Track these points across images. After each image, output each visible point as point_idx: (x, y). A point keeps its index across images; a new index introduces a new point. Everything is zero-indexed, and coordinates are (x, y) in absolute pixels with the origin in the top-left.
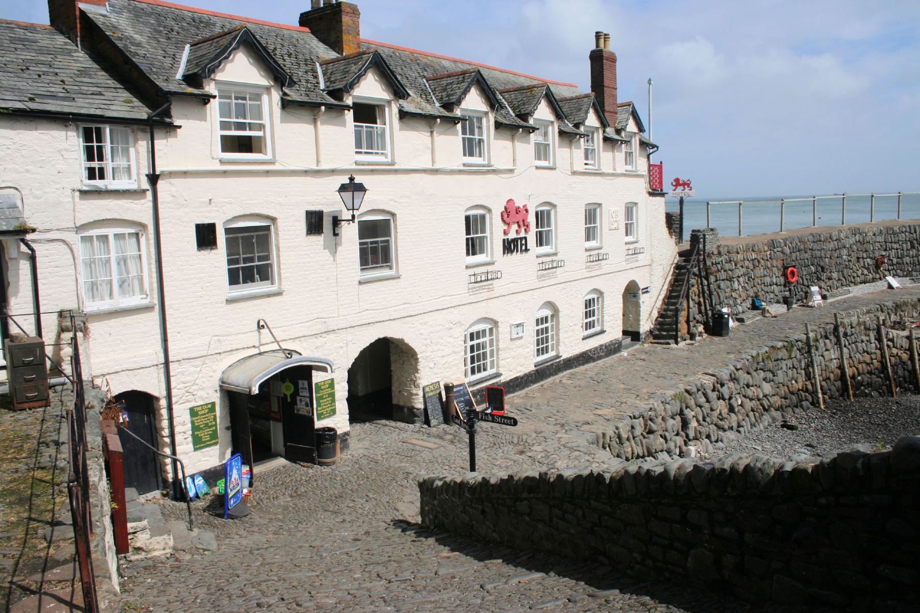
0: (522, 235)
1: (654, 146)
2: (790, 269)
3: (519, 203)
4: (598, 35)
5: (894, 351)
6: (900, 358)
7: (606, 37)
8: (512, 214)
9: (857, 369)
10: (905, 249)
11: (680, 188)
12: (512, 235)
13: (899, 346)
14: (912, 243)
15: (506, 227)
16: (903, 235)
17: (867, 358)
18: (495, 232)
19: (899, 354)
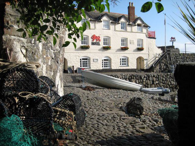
4: (130, 3)
7: (132, 3)
8: (94, 37)
11: (172, 39)
12: (95, 41)
18: (90, 41)
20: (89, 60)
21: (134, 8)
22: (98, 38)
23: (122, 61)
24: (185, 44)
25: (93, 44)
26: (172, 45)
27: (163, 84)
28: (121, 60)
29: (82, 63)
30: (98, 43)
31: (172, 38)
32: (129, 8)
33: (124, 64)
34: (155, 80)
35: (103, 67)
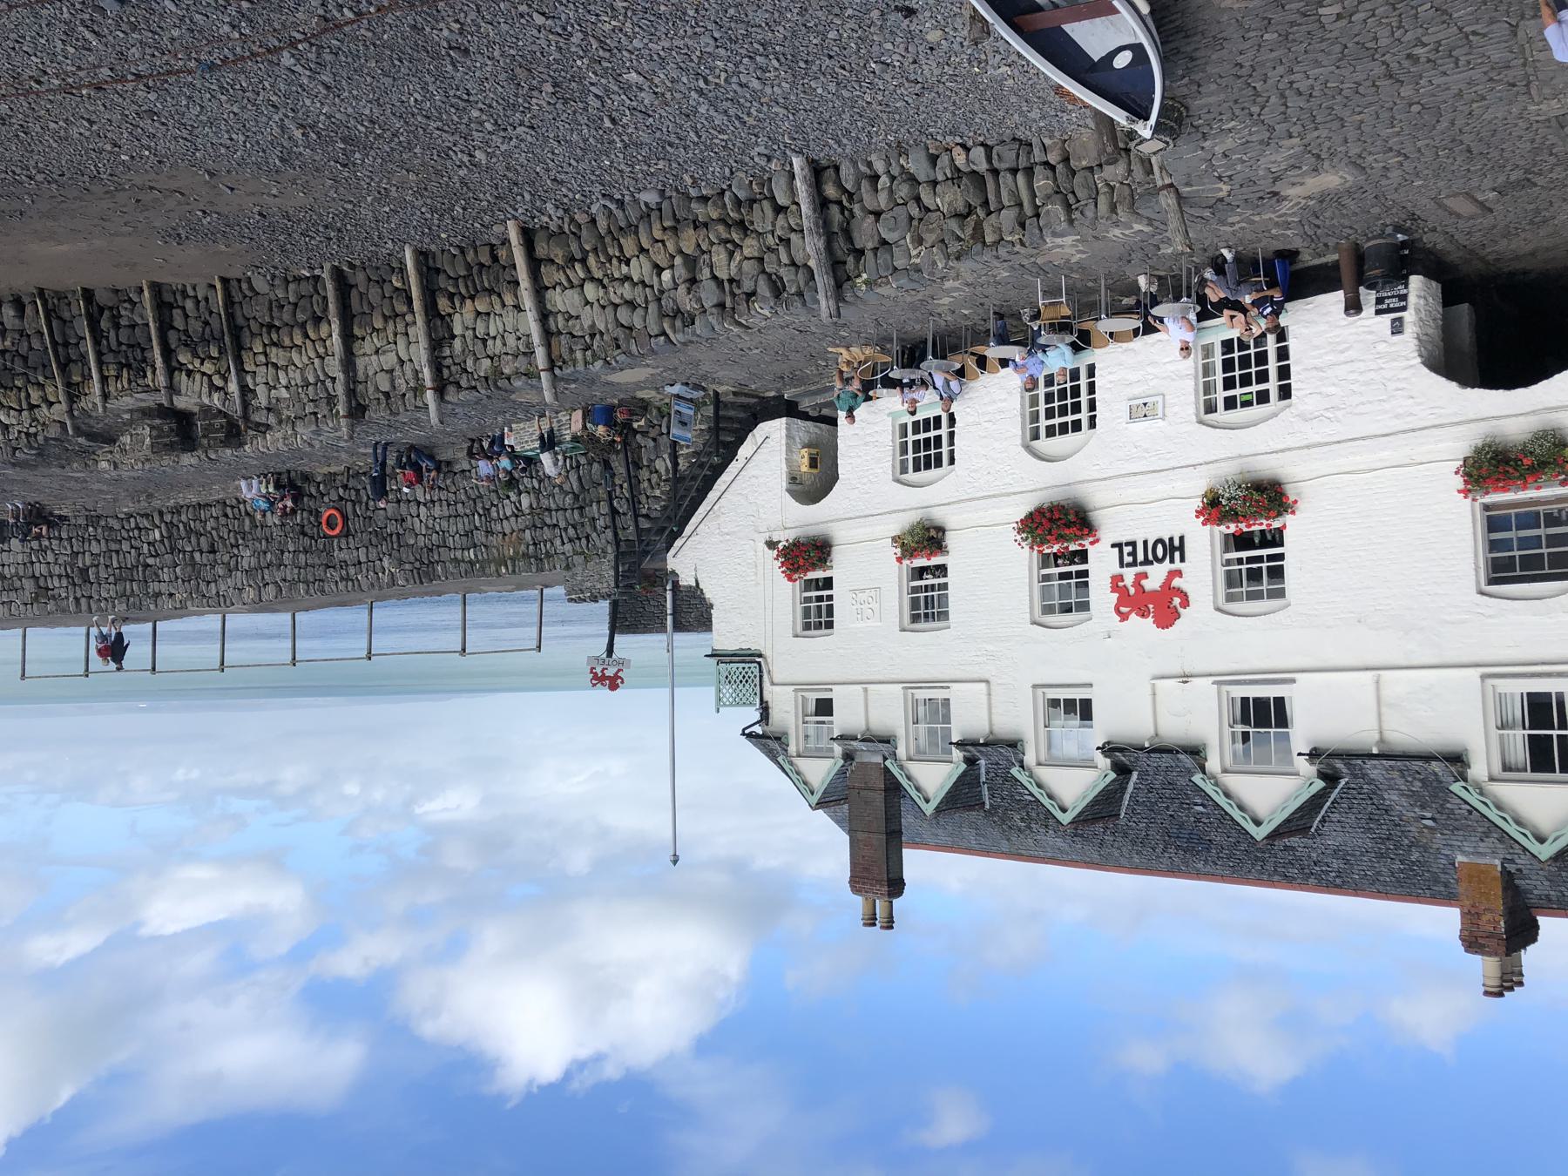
0: (1129, 574)
1: (750, 736)
2: (337, 531)
3: (1143, 626)
4: (889, 924)
5: (208, 367)
6: (195, 355)
7: (871, 921)
9: (306, 336)
10: (102, 568)
11: (610, 672)
12: (1156, 576)
13: (198, 376)
14: (87, 580)
15: (1176, 582)
16: (104, 594)
17: (276, 355)
19: (197, 363)
20: (1210, 408)
21: (859, 880)
22: (1132, 601)
23: (945, 449)
24: (539, 647)
25: (1174, 548)
26: (619, 639)
27: (628, 278)
28: (952, 453)
29: (1272, 366)
30: (1134, 564)
31: (614, 683)
32: (896, 886)
33: (927, 430)
34: (682, 289)
35: (1091, 371)
